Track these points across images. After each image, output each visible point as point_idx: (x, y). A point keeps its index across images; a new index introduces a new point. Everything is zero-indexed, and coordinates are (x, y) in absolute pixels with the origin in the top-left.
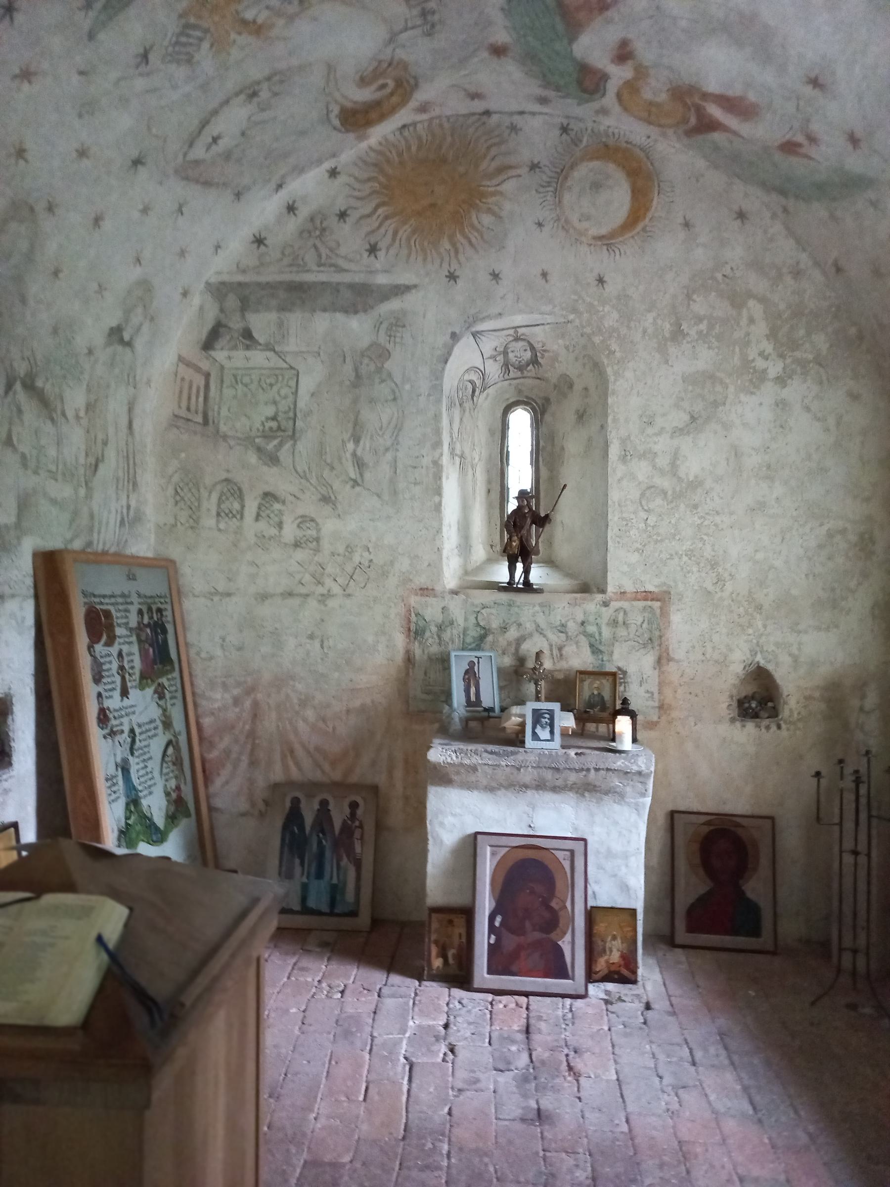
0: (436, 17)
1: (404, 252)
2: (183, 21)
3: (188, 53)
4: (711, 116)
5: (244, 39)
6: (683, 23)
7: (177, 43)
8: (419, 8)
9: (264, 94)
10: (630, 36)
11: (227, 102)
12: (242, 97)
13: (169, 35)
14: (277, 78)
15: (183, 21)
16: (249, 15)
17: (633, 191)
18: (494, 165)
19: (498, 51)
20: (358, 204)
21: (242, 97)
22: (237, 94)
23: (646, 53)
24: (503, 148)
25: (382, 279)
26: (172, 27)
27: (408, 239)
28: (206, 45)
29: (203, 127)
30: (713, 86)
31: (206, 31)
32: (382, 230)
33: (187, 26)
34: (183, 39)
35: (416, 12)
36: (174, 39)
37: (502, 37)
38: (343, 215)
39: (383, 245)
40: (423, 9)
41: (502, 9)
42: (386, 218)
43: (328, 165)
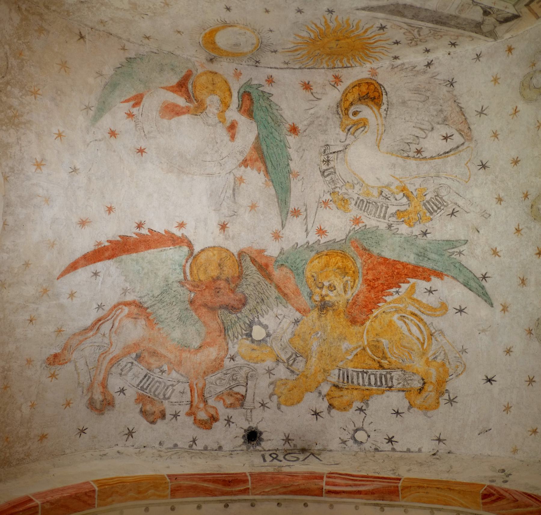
0: (322, 158)
1: (361, 25)
2: (432, 217)
3: (437, 200)
4: (182, 96)
5: (411, 188)
6: (208, 158)
7: (439, 208)
8: (330, 166)
9: (414, 147)
10: (230, 143)
11: (432, 158)
12: (424, 154)
13: (439, 215)
14: (406, 155)
15: (432, 217)
16: (405, 200)
17: (215, 43)
18: (298, 52)
19: (294, 130)
20: (387, 46)
21: (424, 154)
22: (425, 158)
23: (222, 133)
24: (292, 57)
25: (380, 15)
26: (436, 216)
27: (357, 29)
28: (428, 198)
29: (448, 152)
30: (185, 118)
31: (424, 205)
32: (373, 34)
33: (431, 213)
34: (435, 208)
35: (332, 164)
36: (439, 211)
37: (291, 140)
38: (397, 43)
39: (375, 29)
40: (328, 165)
41: (291, 160)
42: (369, 38)
43: (398, 62)
